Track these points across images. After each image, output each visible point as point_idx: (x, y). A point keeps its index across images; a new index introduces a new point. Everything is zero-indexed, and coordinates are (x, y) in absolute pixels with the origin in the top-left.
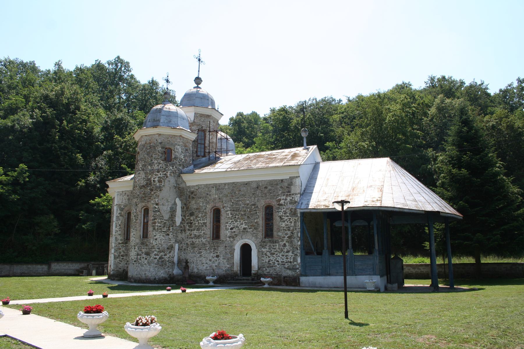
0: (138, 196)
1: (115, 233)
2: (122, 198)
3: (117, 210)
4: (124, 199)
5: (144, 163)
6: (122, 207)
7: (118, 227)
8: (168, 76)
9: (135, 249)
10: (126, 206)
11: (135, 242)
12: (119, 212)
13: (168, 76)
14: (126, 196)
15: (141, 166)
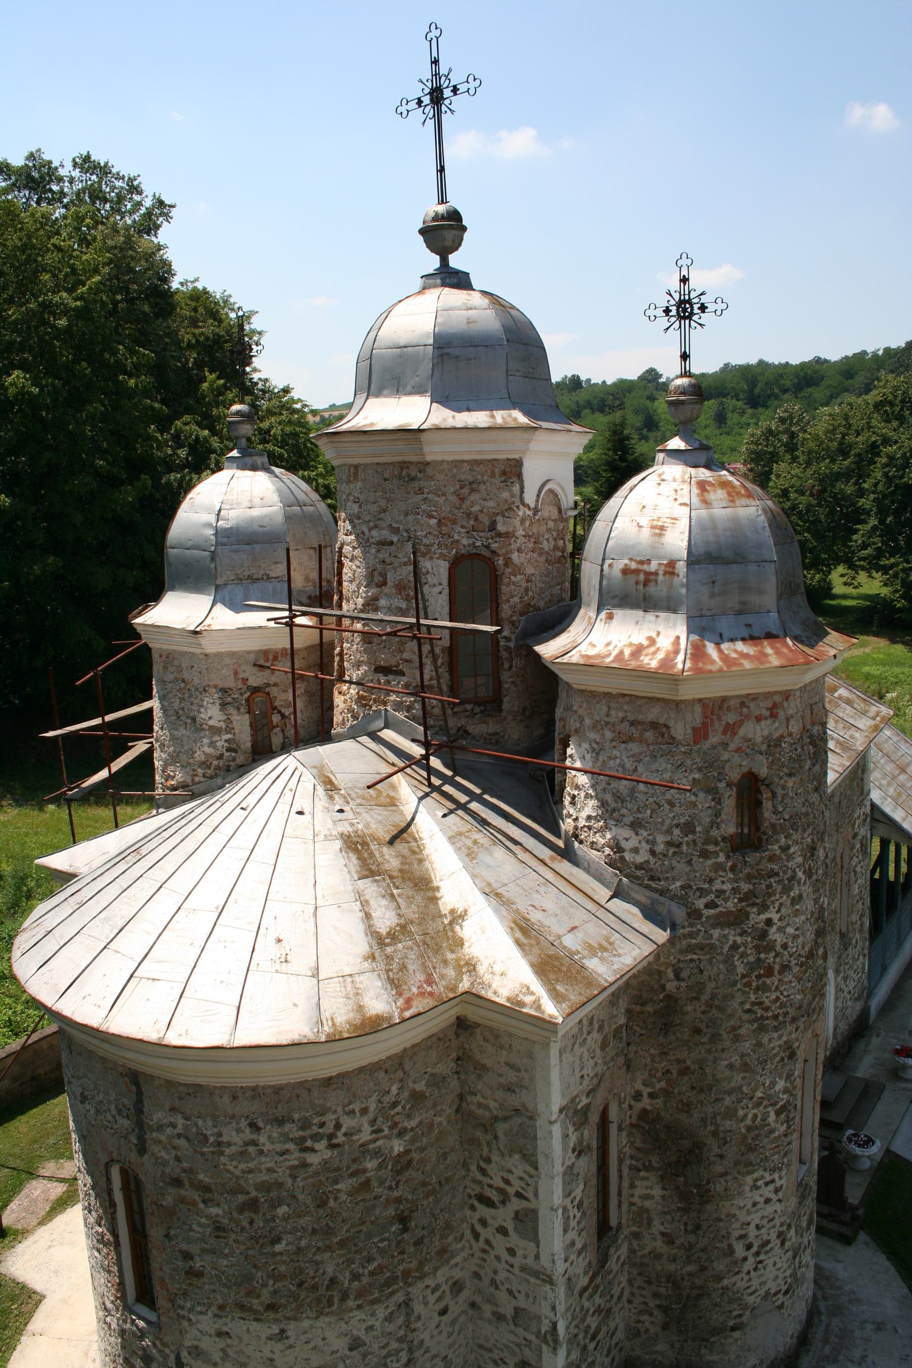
0: (800, 1007)
1: (566, 1261)
2: (581, 1058)
3: (566, 1136)
4: (586, 1055)
5: (809, 840)
6: (585, 1101)
7: (573, 1223)
8: (684, 280)
9: (783, 1244)
10: (598, 1085)
11: (782, 1219)
12: (573, 1139)
13: (684, 280)
14: (595, 1034)
15: (800, 860)
